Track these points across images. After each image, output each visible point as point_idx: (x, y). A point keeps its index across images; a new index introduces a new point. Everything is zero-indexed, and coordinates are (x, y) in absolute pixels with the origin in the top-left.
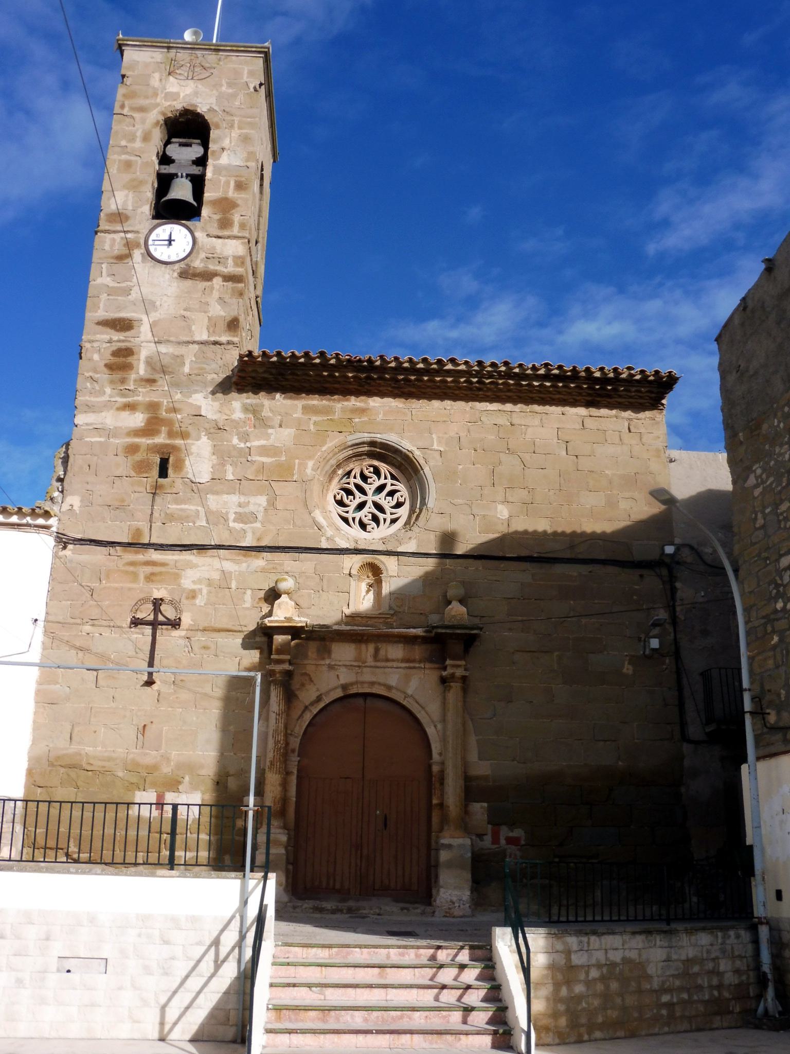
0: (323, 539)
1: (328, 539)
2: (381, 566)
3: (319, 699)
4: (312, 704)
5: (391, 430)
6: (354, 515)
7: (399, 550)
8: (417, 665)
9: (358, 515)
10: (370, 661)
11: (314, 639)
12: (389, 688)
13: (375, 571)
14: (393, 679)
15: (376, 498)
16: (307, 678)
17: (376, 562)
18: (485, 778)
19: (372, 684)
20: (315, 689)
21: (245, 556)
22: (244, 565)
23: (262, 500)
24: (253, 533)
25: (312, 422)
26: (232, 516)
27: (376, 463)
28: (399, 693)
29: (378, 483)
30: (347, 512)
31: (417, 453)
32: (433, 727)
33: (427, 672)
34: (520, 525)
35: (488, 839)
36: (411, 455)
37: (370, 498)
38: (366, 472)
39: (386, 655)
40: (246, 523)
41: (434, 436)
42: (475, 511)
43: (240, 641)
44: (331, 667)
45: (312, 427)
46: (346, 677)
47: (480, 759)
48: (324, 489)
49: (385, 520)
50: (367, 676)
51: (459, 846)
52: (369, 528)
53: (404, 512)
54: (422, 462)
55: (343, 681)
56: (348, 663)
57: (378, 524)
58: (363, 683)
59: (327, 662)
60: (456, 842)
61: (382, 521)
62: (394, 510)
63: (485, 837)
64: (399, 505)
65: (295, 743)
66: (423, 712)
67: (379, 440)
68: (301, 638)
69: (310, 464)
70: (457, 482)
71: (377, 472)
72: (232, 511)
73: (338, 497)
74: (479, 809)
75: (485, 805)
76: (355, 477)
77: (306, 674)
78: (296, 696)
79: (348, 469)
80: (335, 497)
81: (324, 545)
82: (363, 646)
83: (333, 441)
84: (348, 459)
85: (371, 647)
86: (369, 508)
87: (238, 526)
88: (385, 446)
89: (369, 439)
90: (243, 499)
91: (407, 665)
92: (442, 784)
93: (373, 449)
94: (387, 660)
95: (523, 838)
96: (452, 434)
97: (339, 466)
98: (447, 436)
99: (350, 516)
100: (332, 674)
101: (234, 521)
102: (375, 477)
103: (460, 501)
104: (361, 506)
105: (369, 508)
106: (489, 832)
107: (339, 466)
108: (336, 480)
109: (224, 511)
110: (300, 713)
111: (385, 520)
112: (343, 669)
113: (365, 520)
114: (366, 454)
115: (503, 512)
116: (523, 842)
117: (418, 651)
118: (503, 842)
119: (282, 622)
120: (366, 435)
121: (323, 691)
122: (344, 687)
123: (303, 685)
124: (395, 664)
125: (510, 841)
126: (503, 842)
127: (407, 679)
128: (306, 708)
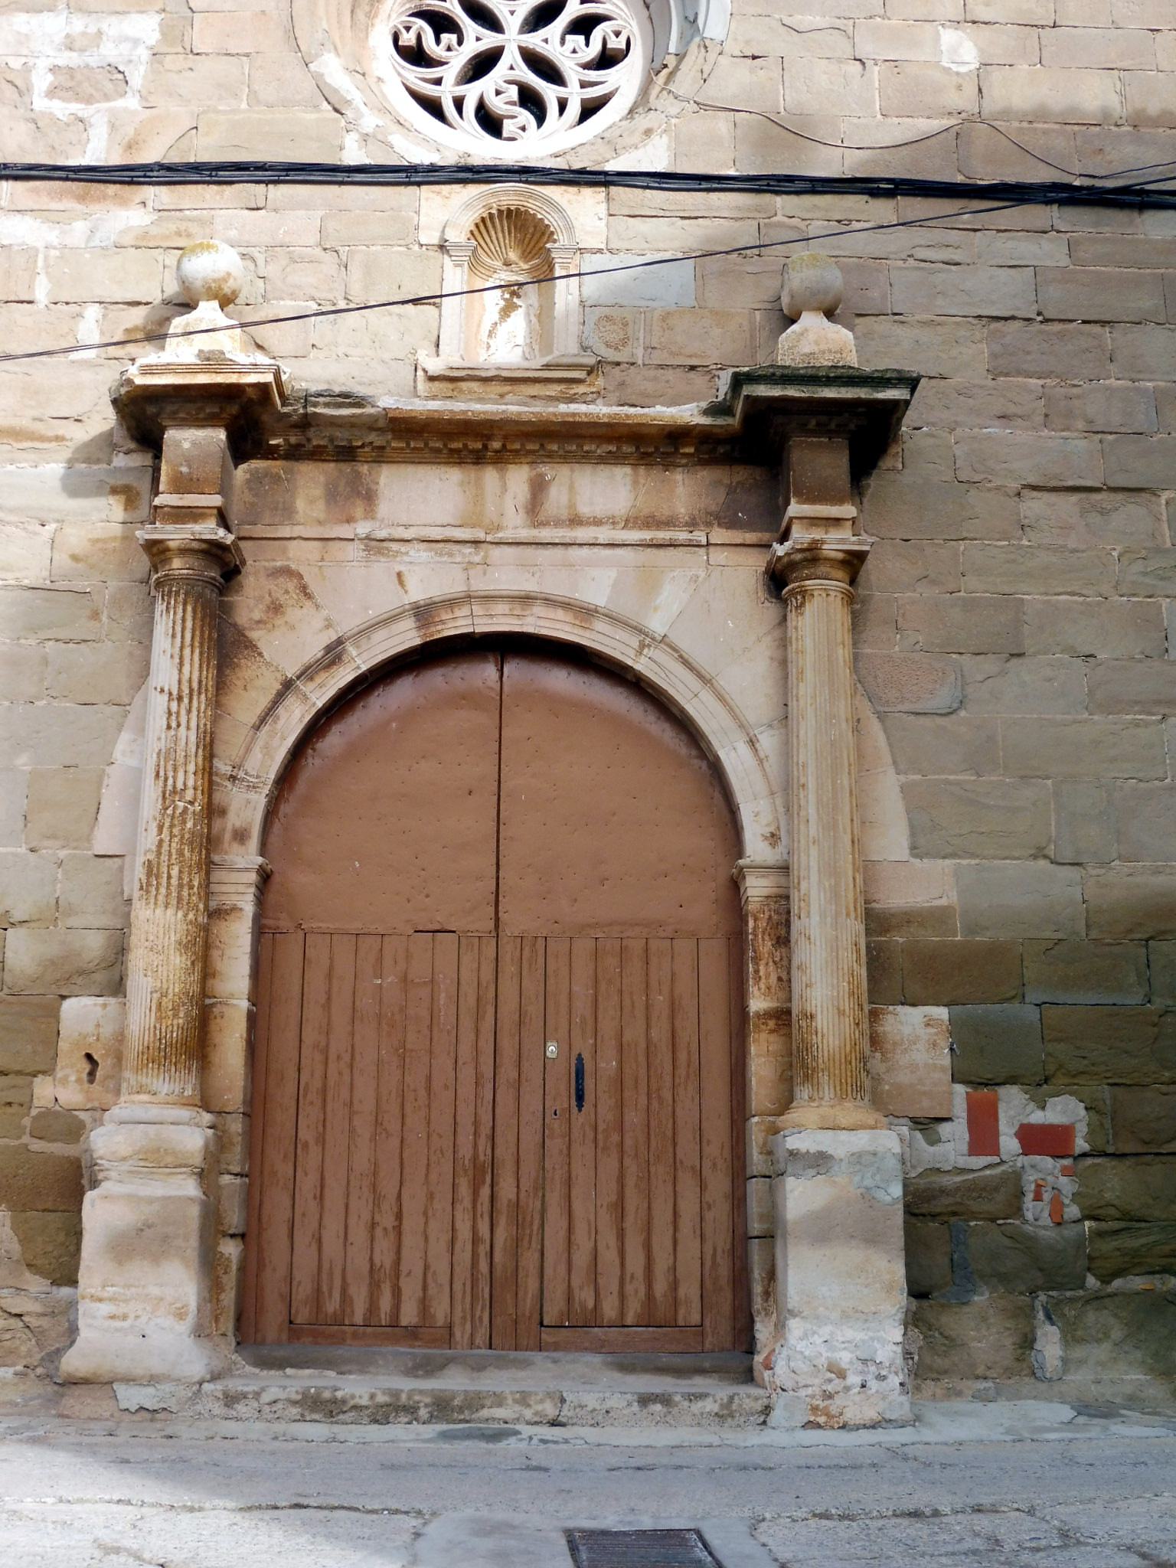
1: (365, 138)
2: (551, 219)
3: (333, 655)
4: (308, 673)
6: (461, 90)
7: (611, 167)
8: (682, 536)
9: (472, 93)
10: (516, 526)
11: (316, 455)
12: (585, 613)
13: (527, 234)
14: (598, 581)
16: (291, 585)
17: (532, 206)
18: (939, 917)
19: (526, 599)
20: (318, 623)
21: (82, 198)
22: (80, 227)
23: (146, 27)
24: (113, 127)
26: (42, 81)
28: (621, 634)
30: (438, 82)
32: (743, 749)
33: (719, 556)
34: (1020, 90)
35: (956, 1134)
37: (512, 39)
39: (572, 506)
40: (89, 100)
42: (865, 50)
43: (54, 469)
44: (375, 545)
46: (428, 578)
47: (915, 850)
48: (361, 31)
49: (562, 105)
50: (506, 574)
51: (858, 1159)
52: (508, 127)
53: (624, 79)
55: (418, 592)
56: (436, 533)
57: (541, 118)
58: (488, 598)
59: (362, 528)
60: (841, 1144)
61: (552, 108)
62: (593, 75)
63: (944, 1129)
64: (607, 60)
65: (246, 807)
66: (706, 695)
68: (271, 453)
72: (43, 64)
73: (408, 39)
74: (920, 1030)
75: (942, 1013)
77: (287, 572)
78: (251, 646)
80: (396, 38)
81: (353, 156)
82: (490, 475)
85: (518, 478)
86: (511, 68)
87: (61, 109)
90: (78, 24)
91: (647, 535)
92: (783, 941)
94: (576, 521)
95: (1082, 1129)
99: (445, 95)
100: (381, 570)
101: (52, 92)
103: (819, 21)
104: (482, 65)
105: (511, 68)
106: (960, 1109)
109: (16, 63)
110: (264, 702)
111: (562, 105)
112: (420, 554)
115: (960, 51)
116: (1081, 1145)
117: (685, 490)
118: (1009, 1143)
119: (189, 369)
121: (347, 625)
122: (423, 613)
123: (276, 608)
124: (604, 534)
125: (1034, 1139)
126: (1009, 1143)
127: (649, 583)
128: (288, 685)
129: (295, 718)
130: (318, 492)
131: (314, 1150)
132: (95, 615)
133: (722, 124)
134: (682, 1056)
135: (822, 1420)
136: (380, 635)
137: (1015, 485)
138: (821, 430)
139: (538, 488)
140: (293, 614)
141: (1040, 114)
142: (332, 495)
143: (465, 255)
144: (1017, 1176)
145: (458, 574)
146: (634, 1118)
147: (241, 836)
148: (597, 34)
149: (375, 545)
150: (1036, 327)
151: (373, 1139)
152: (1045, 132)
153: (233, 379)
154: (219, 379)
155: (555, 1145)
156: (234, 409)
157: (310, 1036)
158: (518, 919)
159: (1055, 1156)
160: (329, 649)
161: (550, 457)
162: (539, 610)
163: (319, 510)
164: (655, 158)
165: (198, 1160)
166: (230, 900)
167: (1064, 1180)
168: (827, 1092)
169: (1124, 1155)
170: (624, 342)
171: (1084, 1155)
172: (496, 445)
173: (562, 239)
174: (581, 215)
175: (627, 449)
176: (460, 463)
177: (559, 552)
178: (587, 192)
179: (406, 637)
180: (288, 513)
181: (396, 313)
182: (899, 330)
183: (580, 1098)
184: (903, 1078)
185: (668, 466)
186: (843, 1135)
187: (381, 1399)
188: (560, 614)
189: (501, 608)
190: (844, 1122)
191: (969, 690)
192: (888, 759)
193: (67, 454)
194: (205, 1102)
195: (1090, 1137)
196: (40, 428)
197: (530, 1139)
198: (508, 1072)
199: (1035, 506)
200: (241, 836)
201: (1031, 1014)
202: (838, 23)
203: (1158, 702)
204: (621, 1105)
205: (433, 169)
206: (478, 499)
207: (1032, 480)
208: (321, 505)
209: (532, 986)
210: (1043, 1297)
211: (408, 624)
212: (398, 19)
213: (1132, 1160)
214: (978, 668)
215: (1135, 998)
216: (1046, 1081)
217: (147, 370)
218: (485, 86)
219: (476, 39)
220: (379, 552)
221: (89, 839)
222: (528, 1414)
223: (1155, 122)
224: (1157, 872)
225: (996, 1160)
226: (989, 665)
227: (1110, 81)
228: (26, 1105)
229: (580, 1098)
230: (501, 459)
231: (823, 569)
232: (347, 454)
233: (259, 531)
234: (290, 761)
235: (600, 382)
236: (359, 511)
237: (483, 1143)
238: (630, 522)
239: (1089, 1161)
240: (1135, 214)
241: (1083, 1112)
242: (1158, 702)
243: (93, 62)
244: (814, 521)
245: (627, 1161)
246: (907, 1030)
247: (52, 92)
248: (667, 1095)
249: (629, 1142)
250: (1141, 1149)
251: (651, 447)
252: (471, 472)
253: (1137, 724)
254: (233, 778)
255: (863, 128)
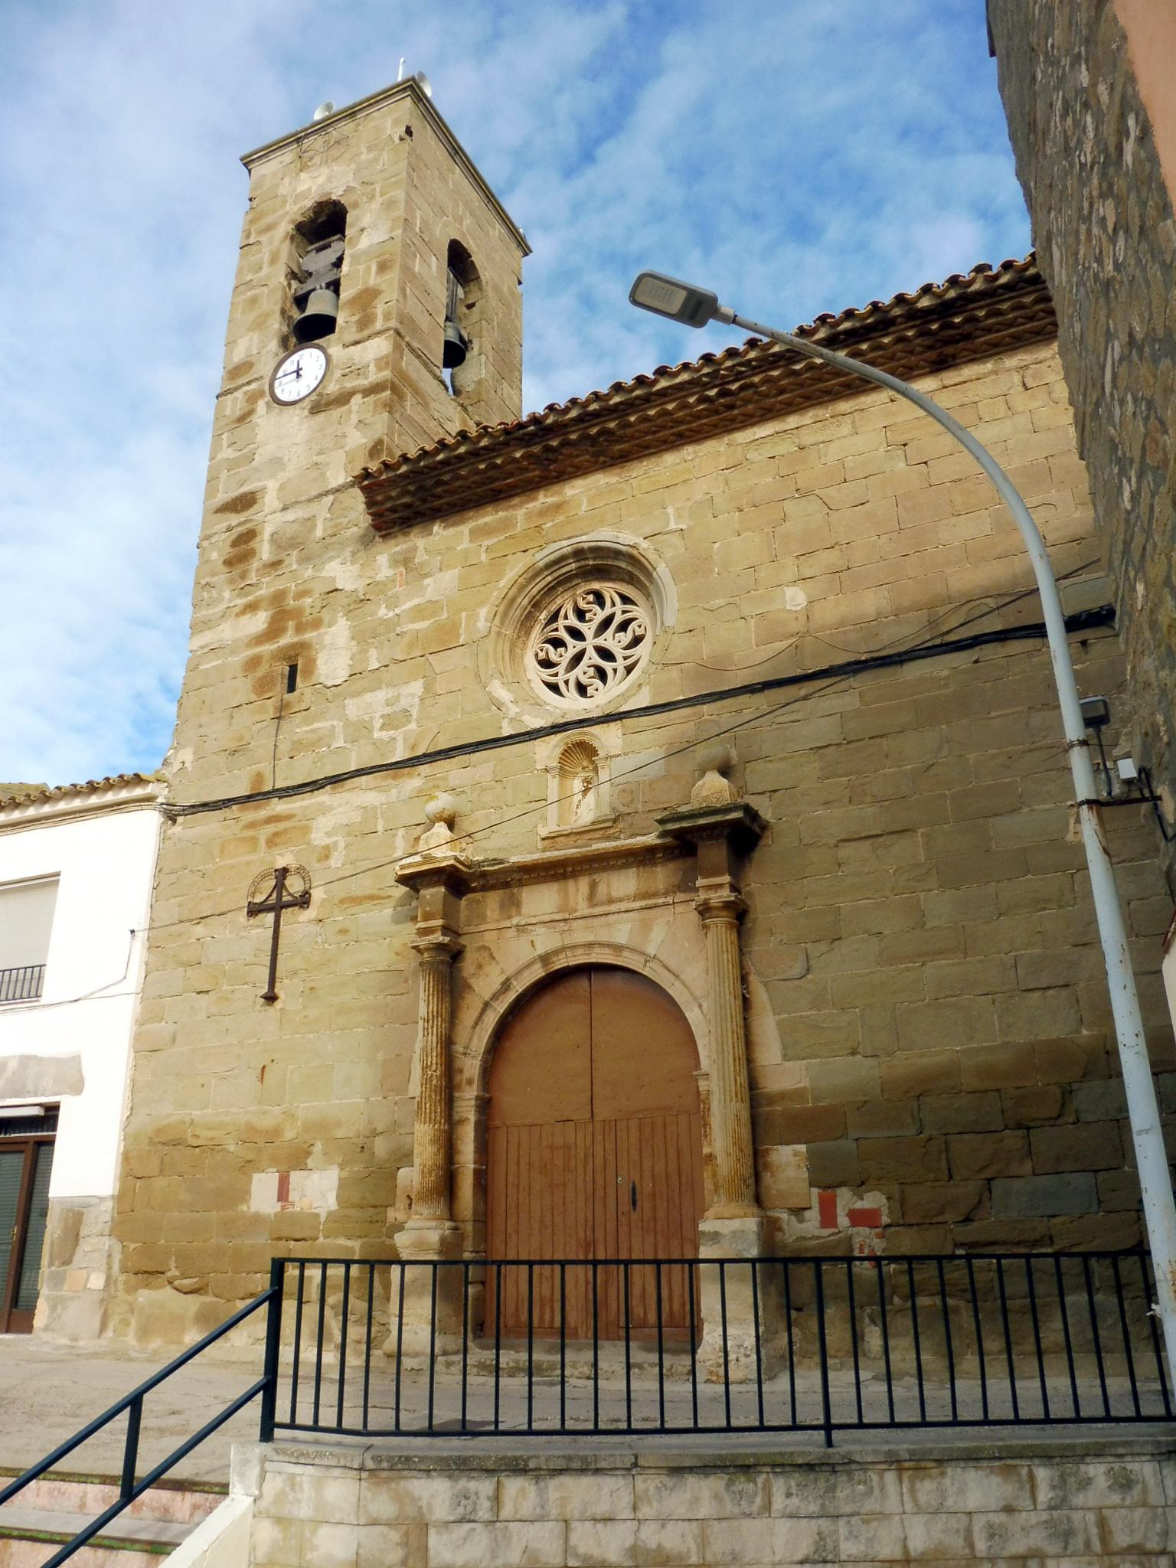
0: (505, 723)
3: (506, 986)
4: (495, 997)
5: (602, 522)
6: (566, 677)
8: (661, 901)
9: (572, 676)
10: (583, 909)
11: (493, 888)
12: (618, 948)
13: (587, 750)
14: (622, 931)
15: (600, 641)
16: (486, 954)
17: (586, 738)
18: (798, 1094)
19: (590, 945)
20: (498, 971)
21: (394, 778)
22: (394, 791)
23: (417, 687)
24: (405, 739)
25: (484, 549)
26: (378, 723)
27: (596, 586)
28: (635, 957)
29: (601, 615)
30: (556, 675)
31: (644, 545)
32: (696, 1009)
33: (679, 909)
34: (830, 612)
35: (813, 1215)
36: (635, 552)
38: (583, 605)
39: (609, 894)
40: (396, 728)
41: (670, 510)
42: (746, 612)
43: (388, 911)
44: (521, 928)
45: (484, 557)
46: (545, 941)
47: (786, 1057)
50: (580, 934)
51: (734, 1234)
54: (652, 556)
55: (541, 950)
56: (547, 918)
58: (573, 947)
59: (515, 921)
60: (726, 1227)
61: (610, 673)
62: (628, 652)
63: (807, 1214)
65: (471, 1067)
66: (677, 984)
67: (586, 545)
68: (474, 890)
69: (483, 612)
70: (712, 571)
71: (600, 599)
72: (378, 715)
73: (542, 656)
74: (789, 1160)
75: (802, 1148)
76: (566, 617)
77: (484, 948)
78: (470, 987)
79: (554, 607)
80: (537, 655)
81: (506, 732)
82: (571, 883)
83: (516, 568)
84: (550, 590)
85: (584, 883)
87: (385, 735)
88: (598, 551)
89: (569, 549)
90: (390, 693)
91: (643, 903)
93: (583, 563)
94: (611, 901)
95: (885, 1211)
96: (699, 496)
97: (536, 605)
98: (690, 503)
99: (559, 680)
100: (524, 941)
101: (382, 729)
102: (596, 608)
104: (578, 658)
106: (815, 1203)
107: (536, 605)
108: (537, 628)
109: (366, 718)
110: (476, 1014)
112: (541, 930)
113: (584, 680)
114: (576, 576)
115: (796, 598)
116: (885, 1219)
117: (662, 875)
118: (843, 1221)
119: (419, 864)
120: (565, 543)
121: (510, 971)
122: (545, 959)
123: (480, 967)
124: (623, 906)
125: (858, 1218)
126: (843, 1221)
127: (646, 928)
128: (486, 1005)
129: (491, 1020)
130: (496, 906)
131: (514, 1237)
132: (406, 981)
133: (674, 673)
134: (684, 1180)
135: (714, 1378)
136: (526, 973)
137: (833, 842)
138: (711, 837)
139: (593, 886)
140: (487, 968)
141: (843, 623)
142: (502, 906)
143: (556, 772)
144: (850, 1238)
145: (558, 937)
146: (661, 1214)
147: (470, 1082)
148: (630, 629)
149: (521, 928)
150: (844, 747)
151: (540, 1231)
152: (844, 632)
153: (437, 865)
154: (432, 866)
155: (623, 1230)
156: (444, 877)
157: (511, 1179)
158: (603, 1112)
159: (871, 1227)
160: (503, 984)
161: (597, 870)
162: (597, 950)
163: (496, 915)
164: (643, 700)
165: (437, 1246)
166: (465, 1115)
167: (876, 1241)
168: (724, 1199)
169: (911, 1225)
170: (632, 802)
171: (889, 1226)
172: (570, 869)
173: (602, 754)
174: (608, 738)
175: (631, 860)
176: (557, 880)
177: (603, 918)
178: (612, 725)
179: (537, 973)
180: (482, 918)
181: (529, 810)
182: (770, 766)
183: (634, 1203)
184: (783, 1186)
185: (654, 864)
186: (727, 1222)
187: (512, 1364)
188: (607, 950)
189: (580, 951)
190: (726, 1215)
191: (812, 962)
192: (768, 1007)
193: (393, 903)
194: (452, 1217)
195: (890, 1213)
196: (382, 893)
197: (611, 1226)
198: (599, 1193)
199: (846, 851)
200: (470, 1082)
201: (853, 1146)
202: (732, 600)
203: (919, 955)
204: (654, 1207)
205: (542, 729)
206: (566, 898)
207: (843, 836)
208: (497, 912)
209: (610, 1146)
210: (868, 1310)
211: (539, 965)
212: (536, 648)
213: (915, 1228)
214: (815, 950)
215: (911, 1131)
216: (863, 1183)
217: (402, 867)
218: (578, 671)
219: (573, 646)
220: (523, 931)
221: (407, 1089)
222: (576, 1373)
223: (908, 610)
224: (922, 1055)
225: (835, 1230)
226: (823, 946)
227: (884, 592)
228: (384, 1221)
229: (634, 1203)
230: (575, 875)
231: (714, 913)
232: (506, 885)
233: (472, 929)
234: (493, 1044)
235: (621, 825)
236: (513, 912)
237: (589, 1233)
238: (636, 898)
239: (893, 1229)
240: (898, 668)
241: (885, 1201)
242: (919, 955)
243: (397, 709)
244: (710, 887)
245: (659, 1238)
246: (784, 1159)
247: (382, 729)
248: (677, 1201)
249: (659, 1227)
250: (920, 1221)
251: (642, 857)
252: (562, 883)
253: (908, 970)
254: (465, 1054)
255: (750, 653)
